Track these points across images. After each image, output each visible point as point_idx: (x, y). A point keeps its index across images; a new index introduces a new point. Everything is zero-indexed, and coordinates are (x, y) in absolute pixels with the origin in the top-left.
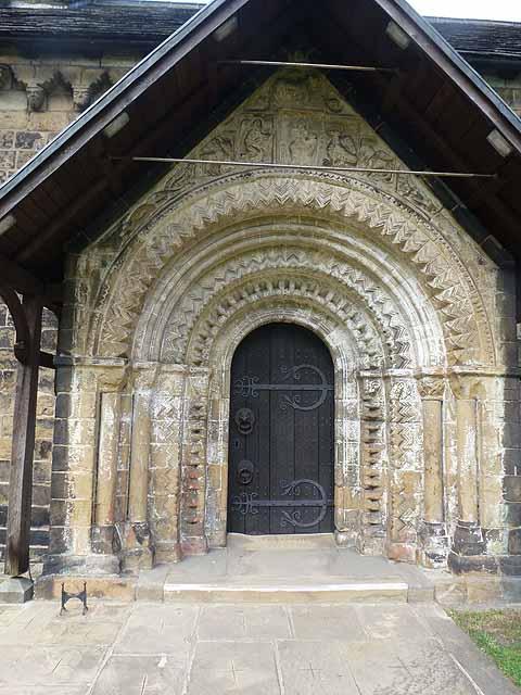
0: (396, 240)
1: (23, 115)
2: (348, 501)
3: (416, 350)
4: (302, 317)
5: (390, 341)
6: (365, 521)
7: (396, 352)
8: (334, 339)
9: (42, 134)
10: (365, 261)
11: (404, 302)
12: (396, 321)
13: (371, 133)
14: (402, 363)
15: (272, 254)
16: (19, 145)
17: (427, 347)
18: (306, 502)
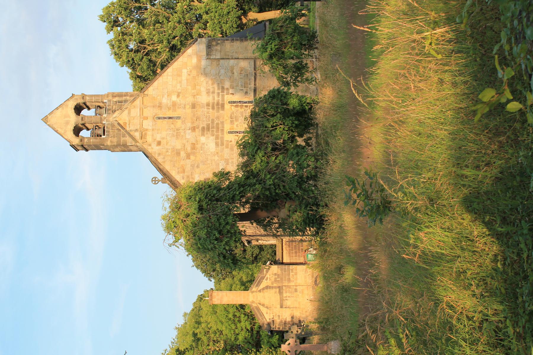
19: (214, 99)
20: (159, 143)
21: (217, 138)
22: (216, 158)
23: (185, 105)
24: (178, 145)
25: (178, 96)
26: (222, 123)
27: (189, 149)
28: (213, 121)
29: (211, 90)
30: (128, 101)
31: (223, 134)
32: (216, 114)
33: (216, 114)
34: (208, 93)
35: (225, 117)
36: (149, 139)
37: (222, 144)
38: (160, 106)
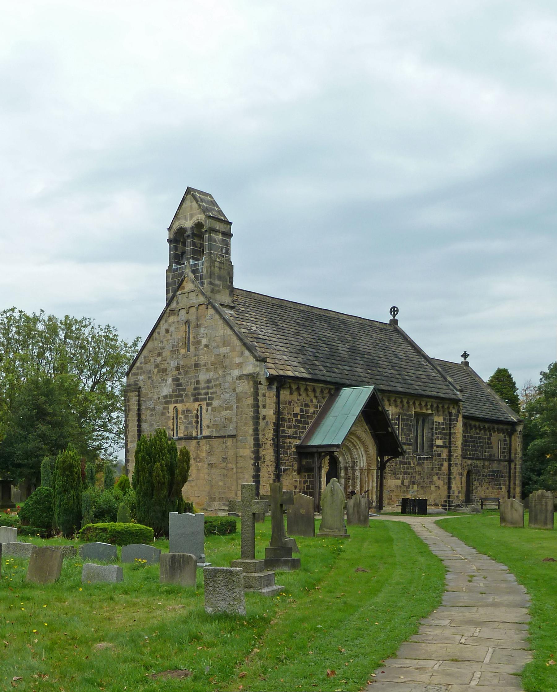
8: (341, 459)
10: (355, 443)
12: (356, 456)
17: (363, 462)
19: (204, 388)
20: (167, 331)
21: (171, 396)
23: (198, 355)
24: (166, 353)
25: (206, 346)
26: (182, 401)
27: (162, 366)
28: (184, 390)
29: (210, 385)
31: (174, 403)
32: (190, 393)
33: (190, 393)
34: (209, 381)
35: (188, 404)
36: (172, 319)
37: (166, 403)
38: (198, 326)
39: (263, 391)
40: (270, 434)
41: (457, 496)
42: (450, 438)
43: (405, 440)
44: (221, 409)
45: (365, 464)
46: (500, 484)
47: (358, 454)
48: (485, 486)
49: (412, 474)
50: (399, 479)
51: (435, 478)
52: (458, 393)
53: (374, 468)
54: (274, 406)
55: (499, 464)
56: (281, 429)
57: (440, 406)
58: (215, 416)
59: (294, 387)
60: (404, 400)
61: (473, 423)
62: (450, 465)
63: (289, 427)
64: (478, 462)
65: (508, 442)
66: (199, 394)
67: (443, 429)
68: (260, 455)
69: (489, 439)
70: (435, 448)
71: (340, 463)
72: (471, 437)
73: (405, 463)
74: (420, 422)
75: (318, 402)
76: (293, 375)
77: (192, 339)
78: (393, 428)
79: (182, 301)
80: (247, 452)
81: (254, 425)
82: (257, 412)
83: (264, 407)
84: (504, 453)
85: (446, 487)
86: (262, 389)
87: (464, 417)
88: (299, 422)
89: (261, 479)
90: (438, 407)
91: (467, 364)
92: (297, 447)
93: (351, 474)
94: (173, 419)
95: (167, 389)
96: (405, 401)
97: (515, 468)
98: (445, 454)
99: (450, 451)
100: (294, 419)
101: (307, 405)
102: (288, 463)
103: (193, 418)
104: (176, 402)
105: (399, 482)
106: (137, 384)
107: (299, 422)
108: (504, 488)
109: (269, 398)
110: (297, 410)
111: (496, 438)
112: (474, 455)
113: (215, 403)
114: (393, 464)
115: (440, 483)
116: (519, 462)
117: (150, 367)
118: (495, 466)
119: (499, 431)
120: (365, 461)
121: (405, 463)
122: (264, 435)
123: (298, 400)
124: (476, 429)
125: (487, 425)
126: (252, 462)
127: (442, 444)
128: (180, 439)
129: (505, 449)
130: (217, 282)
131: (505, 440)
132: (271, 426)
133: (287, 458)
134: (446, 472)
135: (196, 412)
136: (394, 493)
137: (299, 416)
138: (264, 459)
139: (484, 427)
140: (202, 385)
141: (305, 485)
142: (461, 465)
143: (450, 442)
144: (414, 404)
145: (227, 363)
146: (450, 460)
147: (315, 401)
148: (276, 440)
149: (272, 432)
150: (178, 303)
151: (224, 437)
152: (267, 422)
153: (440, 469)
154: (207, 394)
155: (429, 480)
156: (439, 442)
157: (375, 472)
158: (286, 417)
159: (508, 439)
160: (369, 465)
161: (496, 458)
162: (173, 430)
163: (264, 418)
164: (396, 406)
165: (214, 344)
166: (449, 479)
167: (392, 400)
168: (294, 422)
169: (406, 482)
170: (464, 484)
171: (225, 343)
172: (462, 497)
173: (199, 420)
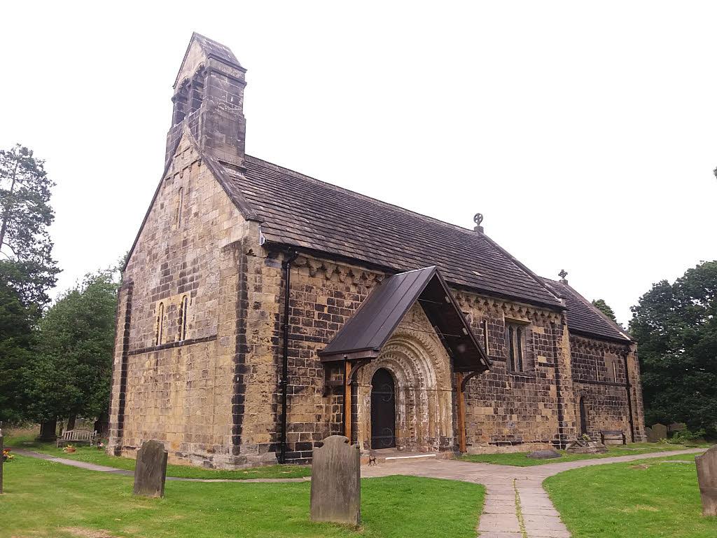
0: (428, 347)
1: (307, 278)
2: (401, 434)
3: (427, 381)
4: (389, 367)
5: (419, 378)
6: (410, 440)
7: (419, 382)
8: (398, 375)
9: (314, 287)
10: (416, 351)
11: (425, 366)
12: (421, 371)
13: (423, 312)
14: (422, 385)
15: (392, 346)
16: (306, 291)
17: (431, 380)
18: (388, 437)
19: (189, 273)
20: (162, 206)
22: (145, 293)
24: (159, 235)
25: (196, 214)
26: (168, 295)
27: (154, 252)
29: (196, 266)
30: (197, 139)
34: (195, 262)
36: (169, 189)
37: (154, 299)
39: (257, 266)
40: (268, 331)
41: (572, 429)
42: (555, 355)
43: (495, 353)
44: (206, 298)
45: (434, 383)
46: (620, 413)
47: (423, 367)
48: (603, 416)
49: (509, 399)
50: (491, 406)
51: (541, 405)
52: (560, 300)
53: (448, 386)
54: (276, 289)
55: (616, 389)
56: (293, 325)
57: (539, 313)
58: (199, 310)
59: (315, 266)
60: (489, 302)
61: (582, 339)
62: (558, 389)
63: (309, 324)
64: (593, 387)
65: (623, 363)
66: (184, 281)
67: (545, 343)
68: (247, 364)
69: (602, 359)
70: (537, 366)
71: (398, 381)
72: (581, 356)
73: (497, 385)
74: (515, 333)
75: (359, 292)
76: (311, 247)
77: (183, 210)
78: (469, 329)
79: (179, 164)
80: (228, 361)
81: (238, 317)
82: (245, 296)
83: (258, 289)
84: (620, 375)
85: (556, 417)
86: (257, 259)
87: (571, 331)
88: (327, 317)
89: (246, 404)
90: (535, 314)
91: (566, 282)
92: (319, 353)
93: (414, 398)
94: (158, 321)
95: (155, 282)
96: (491, 303)
97: (635, 394)
98: (551, 374)
99: (557, 371)
100: (316, 313)
101: (339, 295)
102: (305, 379)
103: (177, 316)
104: (163, 297)
105: (490, 411)
106: (131, 279)
107: (327, 317)
108: (624, 418)
109: (271, 276)
110: (323, 300)
111: (610, 359)
112: (586, 378)
113: (200, 291)
114: (481, 386)
115: (547, 412)
116: (638, 387)
117: (143, 255)
118: (611, 392)
119: (612, 350)
120: (434, 378)
121: (497, 385)
122: (256, 332)
123: (324, 286)
124: (586, 347)
125: (598, 343)
126: (233, 375)
127: (545, 362)
128: (162, 348)
129: (620, 371)
130: (218, 134)
131: (620, 362)
132: (272, 320)
133: (303, 371)
134: (555, 397)
135: (180, 307)
136: (485, 426)
137: (326, 309)
138: (255, 371)
139: (595, 345)
140: (189, 268)
141: (335, 414)
142: (573, 389)
143: (556, 360)
144: (504, 307)
145: (215, 229)
146: (558, 383)
147: (353, 289)
148: (281, 342)
149: (273, 329)
150: (174, 168)
151: (206, 340)
152: (263, 314)
153: (545, 394)
154: (192, 280)
155: (533, 408)
156: (542, 359)
157: (450, 394)
158: (301, 308)
159: (622, 360)
160: (439, 383)
161: (612, 382)
162: (157, 336)
163: (257, 306)
164: (480, 309)
165: (203, 211)
166: (560, 406)
167: (473, 300)
168: (316, 316)
169: (501, 411)
170: (579, 414)
171: (216, 205)
172: (577, 430)
173: (183, 318)
